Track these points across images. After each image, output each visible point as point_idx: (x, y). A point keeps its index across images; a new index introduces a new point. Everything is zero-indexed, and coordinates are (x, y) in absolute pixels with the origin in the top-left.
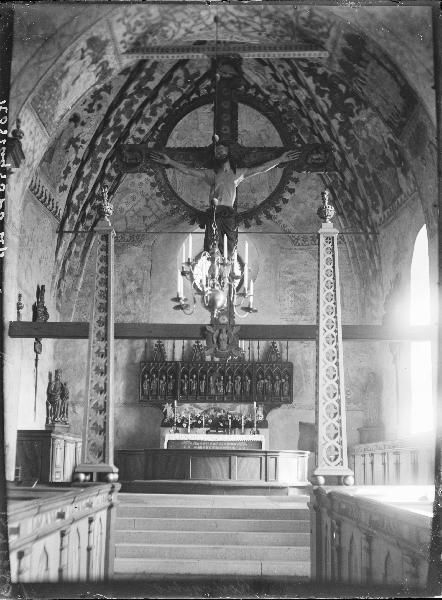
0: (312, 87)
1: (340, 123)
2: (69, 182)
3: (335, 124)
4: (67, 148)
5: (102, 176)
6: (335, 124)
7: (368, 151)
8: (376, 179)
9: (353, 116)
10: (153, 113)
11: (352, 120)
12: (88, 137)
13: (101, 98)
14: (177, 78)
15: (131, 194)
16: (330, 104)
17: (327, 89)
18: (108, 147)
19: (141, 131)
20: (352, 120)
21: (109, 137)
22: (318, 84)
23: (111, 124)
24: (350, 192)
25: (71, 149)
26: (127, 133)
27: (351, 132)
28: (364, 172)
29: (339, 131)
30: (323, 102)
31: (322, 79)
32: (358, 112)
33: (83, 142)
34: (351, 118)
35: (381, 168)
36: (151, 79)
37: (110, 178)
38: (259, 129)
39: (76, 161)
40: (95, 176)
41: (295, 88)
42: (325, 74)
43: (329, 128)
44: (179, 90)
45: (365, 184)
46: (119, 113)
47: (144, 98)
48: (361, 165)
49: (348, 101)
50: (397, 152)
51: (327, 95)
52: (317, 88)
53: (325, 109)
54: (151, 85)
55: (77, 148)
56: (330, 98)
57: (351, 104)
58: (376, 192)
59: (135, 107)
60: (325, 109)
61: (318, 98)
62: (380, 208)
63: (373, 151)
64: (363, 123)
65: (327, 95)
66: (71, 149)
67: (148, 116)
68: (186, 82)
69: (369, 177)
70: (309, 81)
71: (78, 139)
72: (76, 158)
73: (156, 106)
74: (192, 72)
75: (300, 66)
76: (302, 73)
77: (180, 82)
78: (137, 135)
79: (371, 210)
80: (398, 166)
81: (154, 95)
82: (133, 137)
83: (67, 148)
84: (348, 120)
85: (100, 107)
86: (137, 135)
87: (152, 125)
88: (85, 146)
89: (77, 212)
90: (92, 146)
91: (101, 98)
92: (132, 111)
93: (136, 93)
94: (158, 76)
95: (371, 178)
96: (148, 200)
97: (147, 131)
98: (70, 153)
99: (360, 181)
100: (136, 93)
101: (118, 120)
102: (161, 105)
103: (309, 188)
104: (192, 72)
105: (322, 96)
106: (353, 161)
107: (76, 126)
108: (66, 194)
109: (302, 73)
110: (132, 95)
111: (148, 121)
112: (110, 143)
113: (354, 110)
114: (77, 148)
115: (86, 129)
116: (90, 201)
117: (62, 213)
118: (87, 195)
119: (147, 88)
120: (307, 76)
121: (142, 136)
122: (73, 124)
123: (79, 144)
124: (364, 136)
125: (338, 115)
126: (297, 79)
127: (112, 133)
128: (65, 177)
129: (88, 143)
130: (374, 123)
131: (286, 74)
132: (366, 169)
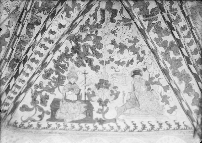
12: (158, 71)
13: (139, 48)
18: (180, 60)
33: (157, 76)
59: (164, 25)
85: (143, 52)
88: (162, 76)
90: (165, 72)
91: (139, 48)
92: (166, 30)
93: (150, 20)
100: (150, 20)
107: (141, 75)
110: (150, 26)
111: (178, 20)
114: (158, 83)
122: (137, 76)
123: (156, 79)
127: (171, 52)
129: (161, 73)
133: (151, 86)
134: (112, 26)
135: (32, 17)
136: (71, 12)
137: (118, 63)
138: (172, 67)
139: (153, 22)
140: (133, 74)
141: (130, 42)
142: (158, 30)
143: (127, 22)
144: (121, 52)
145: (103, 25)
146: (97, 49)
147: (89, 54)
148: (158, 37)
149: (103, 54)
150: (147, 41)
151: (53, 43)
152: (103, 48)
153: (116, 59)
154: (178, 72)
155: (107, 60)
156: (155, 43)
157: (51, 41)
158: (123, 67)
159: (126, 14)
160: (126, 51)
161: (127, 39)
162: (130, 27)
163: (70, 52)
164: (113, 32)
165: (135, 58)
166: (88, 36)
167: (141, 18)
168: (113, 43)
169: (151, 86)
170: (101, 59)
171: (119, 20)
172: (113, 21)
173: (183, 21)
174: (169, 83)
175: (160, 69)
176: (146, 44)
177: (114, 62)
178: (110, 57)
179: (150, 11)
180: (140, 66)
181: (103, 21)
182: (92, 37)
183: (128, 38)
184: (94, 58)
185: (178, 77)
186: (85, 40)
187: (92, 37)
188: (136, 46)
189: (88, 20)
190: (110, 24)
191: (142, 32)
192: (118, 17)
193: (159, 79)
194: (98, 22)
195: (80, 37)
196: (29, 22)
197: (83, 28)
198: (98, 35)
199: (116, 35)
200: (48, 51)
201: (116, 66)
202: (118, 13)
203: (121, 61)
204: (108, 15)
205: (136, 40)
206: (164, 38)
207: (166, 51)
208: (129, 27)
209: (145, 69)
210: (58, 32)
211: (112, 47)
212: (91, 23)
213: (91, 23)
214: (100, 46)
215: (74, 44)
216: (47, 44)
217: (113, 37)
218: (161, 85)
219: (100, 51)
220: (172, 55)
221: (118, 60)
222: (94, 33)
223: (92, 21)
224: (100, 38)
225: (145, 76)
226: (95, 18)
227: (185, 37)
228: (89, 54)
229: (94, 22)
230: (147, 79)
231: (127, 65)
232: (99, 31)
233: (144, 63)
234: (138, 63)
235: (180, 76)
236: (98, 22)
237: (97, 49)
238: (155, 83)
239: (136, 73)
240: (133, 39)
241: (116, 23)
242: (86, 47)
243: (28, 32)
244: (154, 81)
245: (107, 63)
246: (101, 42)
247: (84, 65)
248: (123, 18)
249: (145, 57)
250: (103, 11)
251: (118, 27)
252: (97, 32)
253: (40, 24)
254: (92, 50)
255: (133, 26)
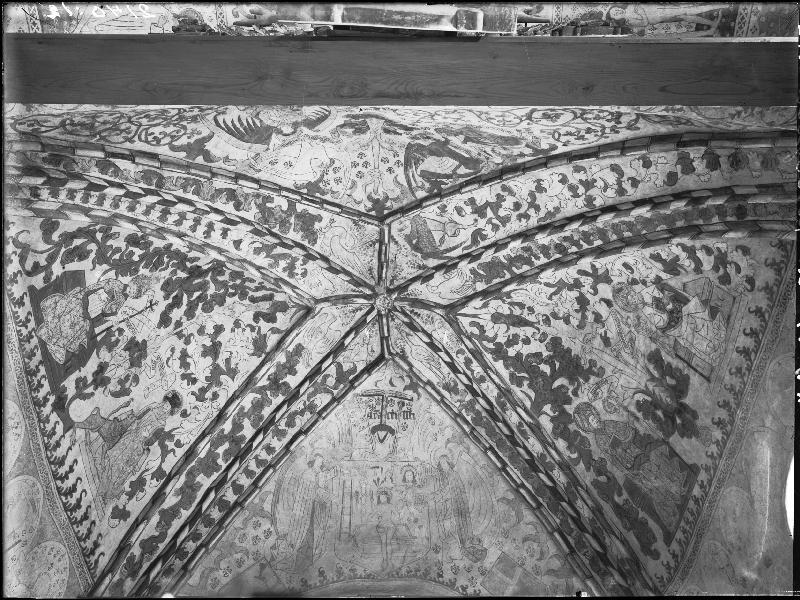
0: (505, 374)
1: (553, 419)
2: (136, 507)
3: (546, 423)
4: (149, 443)
5: (197, 514)
6: (546, 423)
7: (607, 447)
8: (633, 490)
9: (569, 401)
10: (290, 424)
11: (570, 409)
12: (188, 440)
14: (328, 376)
15: (238, 556)
16: (533, 395)
17: (526, 376)
18: (217, 467)
19: (269, 449)
20: (570, 409)
21: (221, 450)
22: (512, 370)
23: (227, 426)
24: (594, 536)
25: (156, 448)
26: (249, 449)
27: (572, 427)
28: (608, 488)
29: (553, 432)
30: (523, 393)
31: (517, 362)
32: (575, 393)
33: (179, 444)
34: (566, 407)
35: (637, 464)
36: (293, 372)
37: (209, 522)
38: (439, 454)
39: (158, 474)
40: (185, 514)
41: (482, 380)
42: (519, 355)
43: (536, 429)
44: (328, 392)
45: (617, 508)
46: (242, 414)
47: (281, 398)
48: (603, 479)
49: (557, 384)
50: (659, 413)
51: (526, 383)
52: (512, 376)
53: (528, 404)
54: (293, 381)
55: (165, 452)
56: (530, 386)
57: (562, 386)
58: (642, 514)
59: (267, 412)
60: (528, 404)
61: (514, 388)
62: (659, 545)
63: (615, 444)
64: (588, 405)
65: (526, 383)
66: (156, 448)
67: (282, 426)
68: (339, 381)
69: (620, 495)
70: (499, 365)
71: (170, 435)
72: (160, 467)
73: (296, 413)
74: (346, 367)
75: (486, 349)
76: (488, 357)
77: (331, 381)
78: (264, 455)
79: (641, 556)
80: (669, 434)
81: (294, 396)
82: (256, 458)
83: (149, 443)
84: (563, 412)
85: (215, 396)
86: (264, 455)
87: (286, 440)
88: (180, 452)
89: (133, 574)
90: (191, 453)
91: (219, 384)
92: (261, 418)
94: (303, 370)
95: (625, 495)
96: (263, 567)
97: (278, 450)
98: (151, 457)
99: (607, 508)
100: (269, 387)
101: (237, 426)
102: (302, 413)
103: (525, 540)
104: (346, 367)
105: (520, 385)
106: (586, 476)
108: (124, 526)
109: (488, 357)
110: (263, 389)
111: (280, 434)
112: (220, 461)
113: (570, 393)
114: (165, 452)
115: (188, 425)
116: (164, 557)
117: (104, 562)
118: (162, 546)
119: (285, 384)
120: (495, 360)
121: (269, 458)
122: (168, 407)
123: (170, 445)
124: (594, 424)
125: (547, 408)
126: (485, 367)
127: (226, 445)
128: (131, 495)
129: (186, 447)
130: (605, 395)
131: (468, 362)
132: (611, 479)
133: (156, 443)
134: (247, 318)
135: (247, 194)
136: (263, 254)
137: (184, 355)
138: (201, 461)
139: (268, 393)
140: (170, 396)
141: (228, 361)
142: (258, 406)
143: (259, 345)
144: (204, 354)
145: (247, 302)
146: (200, 305)
147: (190, 295)
148: (246, 411)
149: (194, 320)
150: (237, 398)
151: (205, 238)
152: (205, 314)
153: (190, 349)
154: (195, 477)
155: (185, 332)
156: (236, 411)
157: (207, 234)
158: (179, 370)
159: (272, 340)
160: (209, 360)
161: (231, 353)
162: (253, 355)
163: (188, 265)
164: (237, 324)
165: (202, 383)
166: (224, 284)
167: (272, 370)
168: (219, 329)
169: (156, 443)
170: (184, 319)
171: (259, 328)
172: (256, 317)
173: (280, 444)
174: (170, 473)
175: (192, 442)
176: (230, 395)
177: (184, 346)
178: (192, 334)
179: (285, 380)
180: (188, 401)
181: (253, 300)
182: (222, 291)
183: (235, 354)
184: (184, 307)
185: (185, 483)
186: (215, 281)
187: (222, 291)
188: (223, 378)
189: (252, 281)
190: (251, 314)
191: (250, 380)
192: (264, 326)
193: (173, 451)
194: (251, 293)
195: (222, 273)
196: (239, 192)
197: (235, 275)
198: (228, 299)
199: (233, 330)
200: (189, 233)
201: (178, 354)
202: (271, 325)
203: (189, 360)
204: (265, 307)
205: (232, 373)
206: (247, 423)
207: (226, 436)
208: (252, 352)
209: (184, 414)
210: (226, 241)
211: (210, 330)
212: (247, 284)
213: (247, 284)
214: (208, 309)
215: (205, 268)
216: (201, 229)
217: (229, 325)
218: (163, 461)
219: (199, 311)
220: (221, 450)
221: (189, 352)
222: (231, 291)
223: (252, 285)
224: (221, 303)
225: (171, 422)
226: (257, 289)
227: (256, 458)
228: (190, 295)
229: (250, 288)
230: (167, 430)
231: (184, 377)
232: (236, 298)
233: (195, 407)
234: (193, 393)
235: (189, 484)
236: (251, 293)
237: (200, 305)
238: (163, 447)
239: (174, 400)
240: (233, 366)
241: (254, 324)
242: (203, 287)
243: (219, 191)
244: (167, 443)
245: (180, 335)
246: (216, 307)
247: (166, 297)
248: (265, 335)
249: (207, 403)
250: (270, 298)
251: (248, 329)
252: (233, 295)
253: (238, 210)
254: (199, 297)
255: (257, 361)
